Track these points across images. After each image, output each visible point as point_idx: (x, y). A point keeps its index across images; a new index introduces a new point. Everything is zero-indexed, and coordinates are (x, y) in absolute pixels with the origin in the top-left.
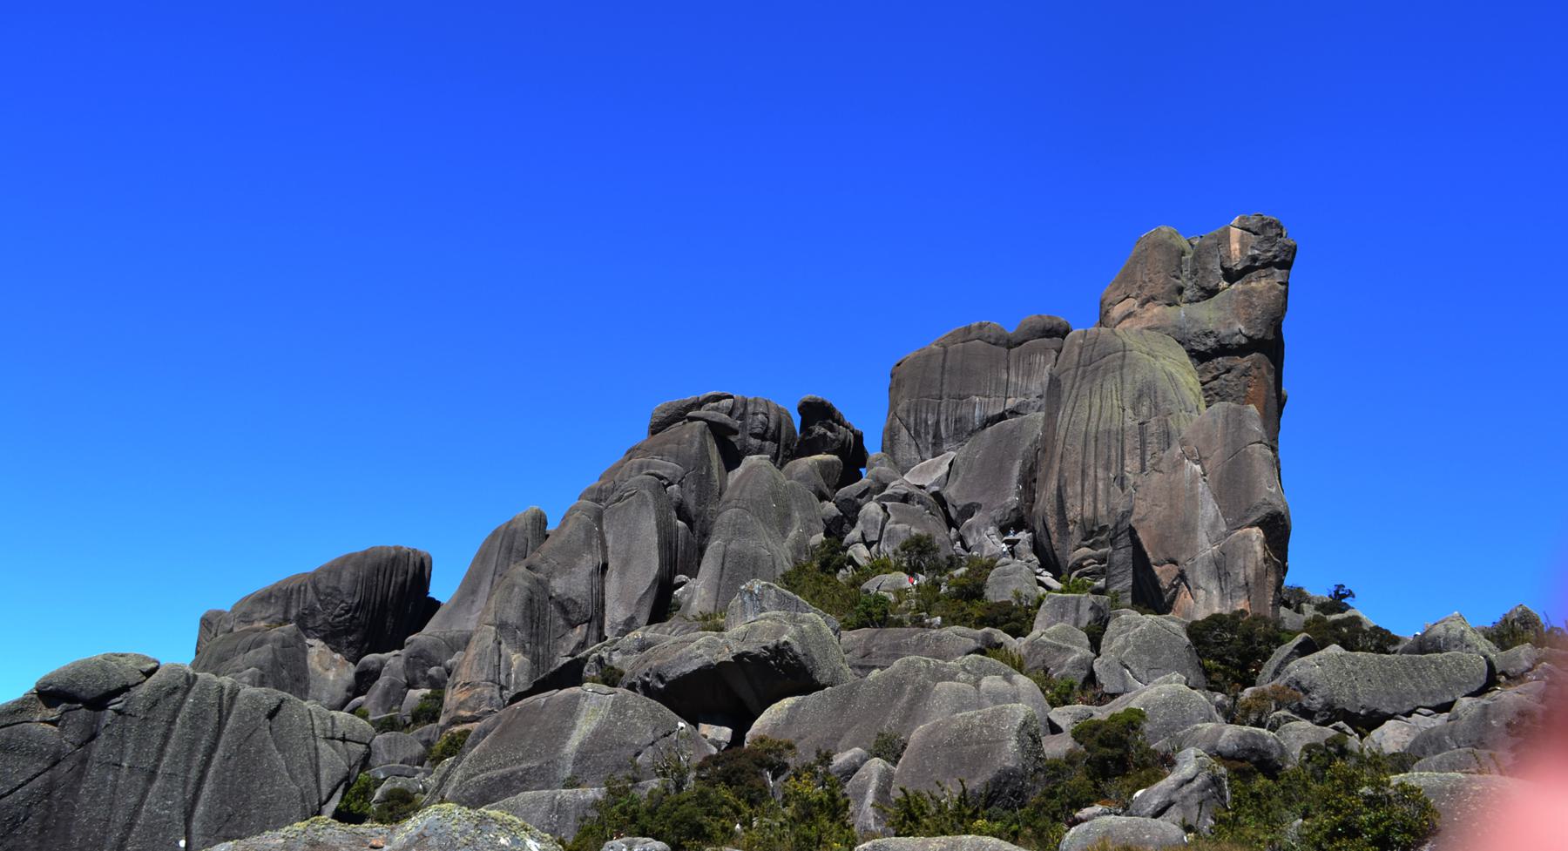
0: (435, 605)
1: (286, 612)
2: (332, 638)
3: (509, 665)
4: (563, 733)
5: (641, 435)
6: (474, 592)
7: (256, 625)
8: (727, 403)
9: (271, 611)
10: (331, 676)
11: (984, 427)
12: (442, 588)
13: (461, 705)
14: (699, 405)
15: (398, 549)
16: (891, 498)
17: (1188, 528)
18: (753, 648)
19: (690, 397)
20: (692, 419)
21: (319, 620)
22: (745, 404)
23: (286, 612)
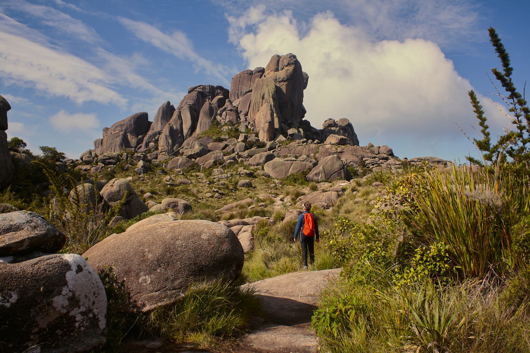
0: (150, 123)
1: (122, 129)
2: (132, 134)
3: (169, 142)
4: (177, 162)
5: (186, 94)
6: (158, 121)
7: (116, 132)
8: (202, 87)
9: (119, 129)
10: (133, 140)
11: (246, 94)
12: (150, 120)
13: (162, 149)
14: (196, 88)
15: (141, 113)
16: (228, 110)
17: (261, 123)
18: (195, 153)
19: (195, 86)
20: (195, 91)
21: (129, 130)
22: (205, 87)
23: (122, 129)
